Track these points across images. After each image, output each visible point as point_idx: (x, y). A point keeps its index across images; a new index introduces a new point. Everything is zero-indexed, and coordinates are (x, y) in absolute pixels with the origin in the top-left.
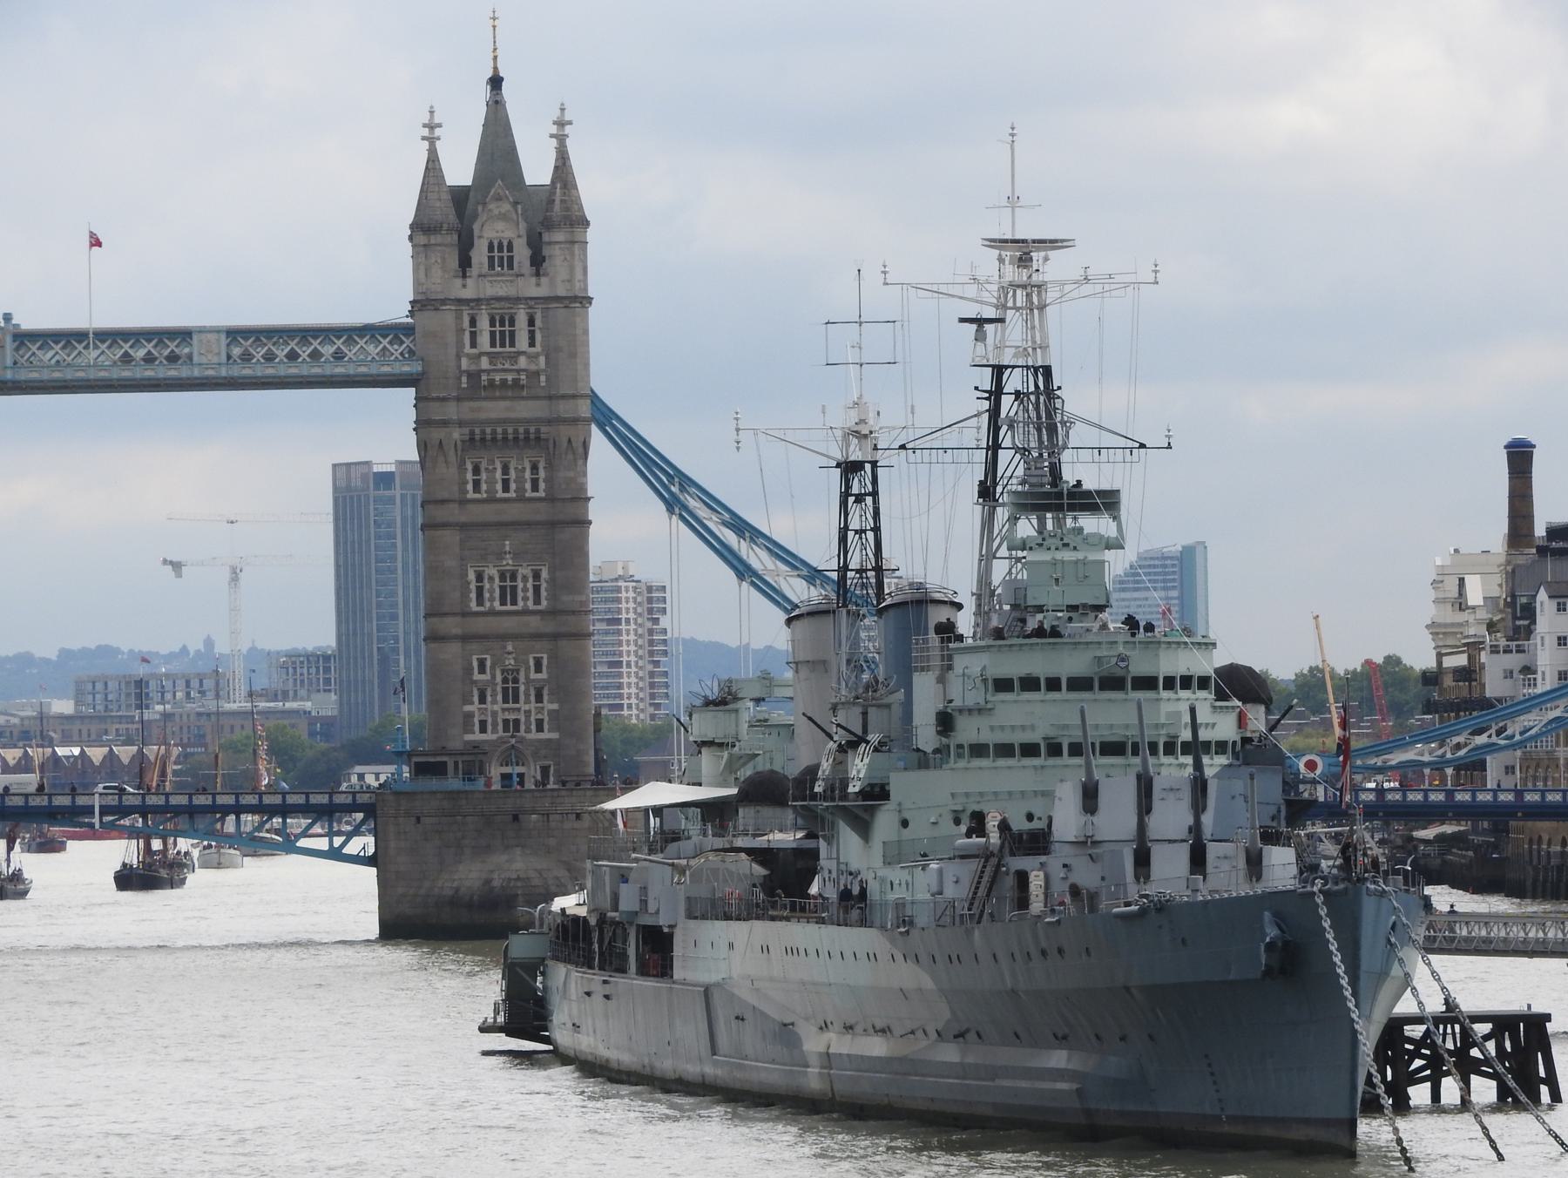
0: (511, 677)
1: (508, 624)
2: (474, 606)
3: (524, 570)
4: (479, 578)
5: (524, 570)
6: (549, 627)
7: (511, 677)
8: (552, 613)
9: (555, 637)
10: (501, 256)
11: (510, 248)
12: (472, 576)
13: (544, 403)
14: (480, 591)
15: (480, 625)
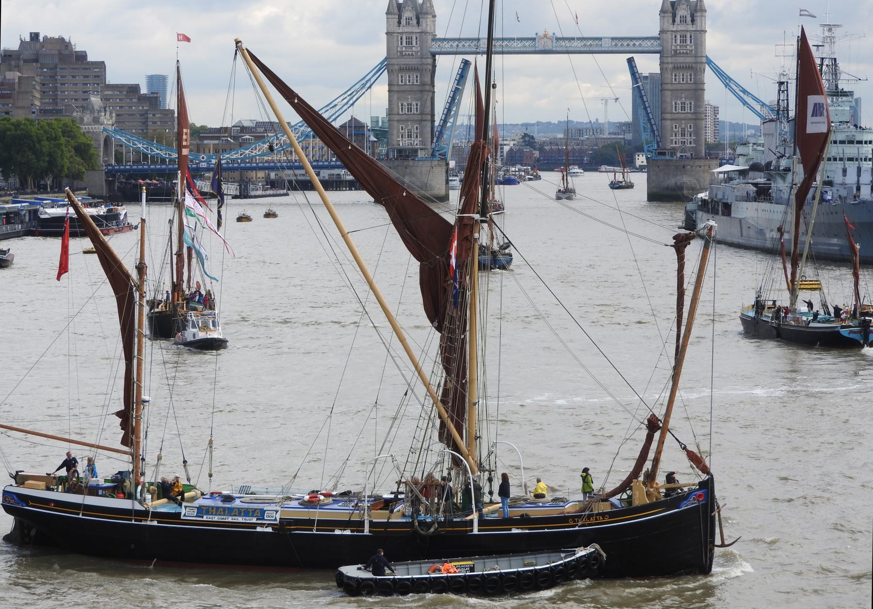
0: (683, 130)
1: (683, 116)
2: (674, 111)
3: (688, 102)
4: (676, 104)
5: (688, 102)
6: (694, 117)
7: (683, 130)
8: (695, 113)
9: (695, 119)
10: (683, 20)
11: (686, 18)
12: (674, 103)
13: (694, 58)
14: (676, 107)
15: (675, 116)
